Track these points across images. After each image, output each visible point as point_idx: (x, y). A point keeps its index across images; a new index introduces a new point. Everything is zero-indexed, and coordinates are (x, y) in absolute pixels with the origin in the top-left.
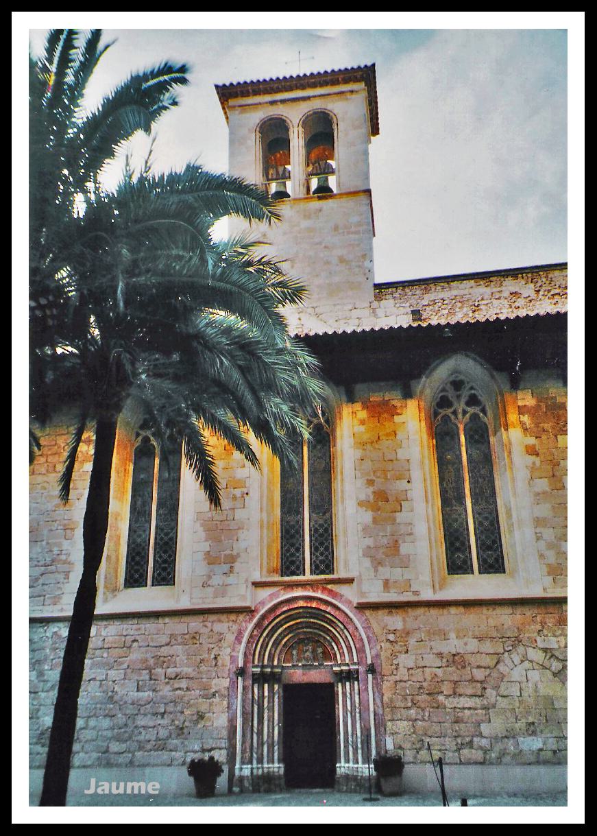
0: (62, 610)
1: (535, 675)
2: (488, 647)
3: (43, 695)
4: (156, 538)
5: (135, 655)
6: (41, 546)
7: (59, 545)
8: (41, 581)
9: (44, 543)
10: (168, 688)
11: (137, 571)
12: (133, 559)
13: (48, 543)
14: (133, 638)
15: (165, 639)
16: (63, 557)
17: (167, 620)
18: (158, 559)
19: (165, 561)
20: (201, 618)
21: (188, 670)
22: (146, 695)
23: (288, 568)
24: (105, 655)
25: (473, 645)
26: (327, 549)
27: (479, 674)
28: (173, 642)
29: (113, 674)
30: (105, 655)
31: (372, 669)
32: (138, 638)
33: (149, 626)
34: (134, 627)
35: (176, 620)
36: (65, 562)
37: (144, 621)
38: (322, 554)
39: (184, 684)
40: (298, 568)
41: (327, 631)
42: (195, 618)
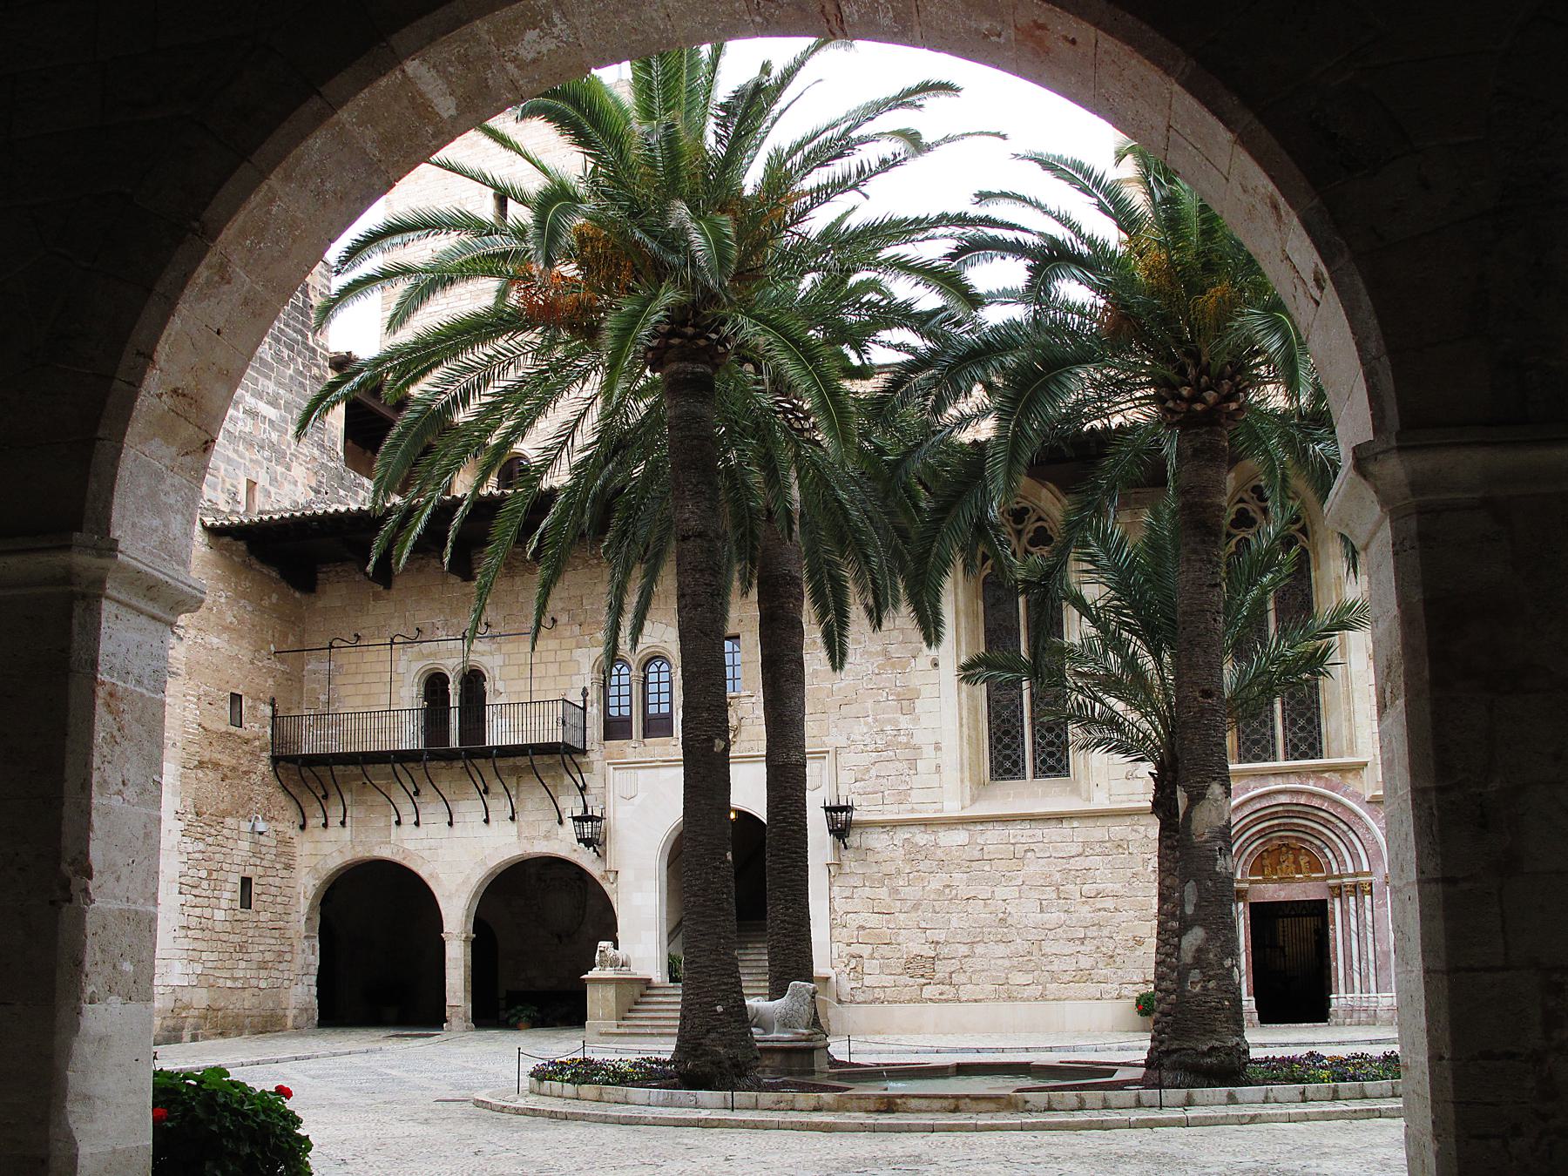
0: (912, 811)
3: (902, 916)
4: (1032, 711)
5: (1033, 868)
6: (866, 724)
7: (895, 722)
8: (873, 772)
9: (870, 719)
10: (1087, 908)
11: (1007, 757)
12: (999, 740)
13: (876, 720)
14: (1026, 847)
15: (1075, 849)
16: (903, 739)
17: (1075, 824)
18: (1038, 739)
19: (1051, 744)
20: (1128, 821)
21: (1109, 887)
22: (1054, 917)
23: (1248, 750)
24: (987, 868)
26: (1310, 721)
28: (1088, 851)
29: (1001, 892)
30: (987, 868)
32: (1033, 846)
33: (1052, 832)
34: (1031, 832)
35: (1090, 823)
36: (907, 746)
37: (1041, 825)
38: (1302, 729)
39: (1109, 903)
40: (1265, 749)
41: (1317, 835)
42: (1118, 820)
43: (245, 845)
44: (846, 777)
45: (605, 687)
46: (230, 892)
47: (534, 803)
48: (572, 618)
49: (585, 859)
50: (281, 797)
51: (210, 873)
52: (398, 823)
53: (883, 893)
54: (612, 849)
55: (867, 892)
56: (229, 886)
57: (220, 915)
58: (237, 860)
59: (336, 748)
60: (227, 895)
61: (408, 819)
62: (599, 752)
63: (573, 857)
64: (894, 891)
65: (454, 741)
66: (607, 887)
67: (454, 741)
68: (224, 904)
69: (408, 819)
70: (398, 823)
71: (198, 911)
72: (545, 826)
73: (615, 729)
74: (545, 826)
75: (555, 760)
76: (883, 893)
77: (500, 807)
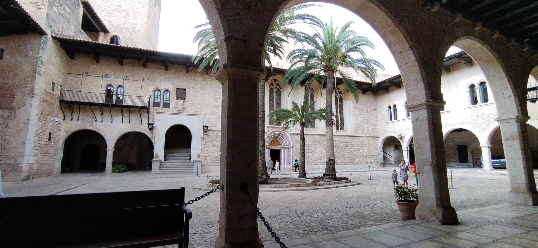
1: (322, 149)
2: (314, 143)
25: (312, 143)
27: (312, 149)
31: (292, 147)
43: (51, 124)
44: (206, 120)
45: (154, 95)
46: (46, 137)
47: (135, 118)
48: (148, 79)
49: (148, 133)
50: (60, 111)
51: (43, 131)
52: (96, 121)
53: (211, 144)
54: (155, 131)
55: (208, 143)
56: (46, 135)
57: (43, 143)
58: (49, 128)
59: (77, 100)
60: (46, 137)
61: (99, 119)
62: (152, 109)
63: (144, 132)
64: (213, 144)
65: (114, 103)
66: (152, 140)
67: (114, 103)
68: (45, 140)
69: (99, 119)
70: (96, 121)
71: (38, 142)
72: (137, 125)
73: (157, 105)
74: (137, 125)
75: (141, 110)
76: (211, 144)
77: (126, 119)
